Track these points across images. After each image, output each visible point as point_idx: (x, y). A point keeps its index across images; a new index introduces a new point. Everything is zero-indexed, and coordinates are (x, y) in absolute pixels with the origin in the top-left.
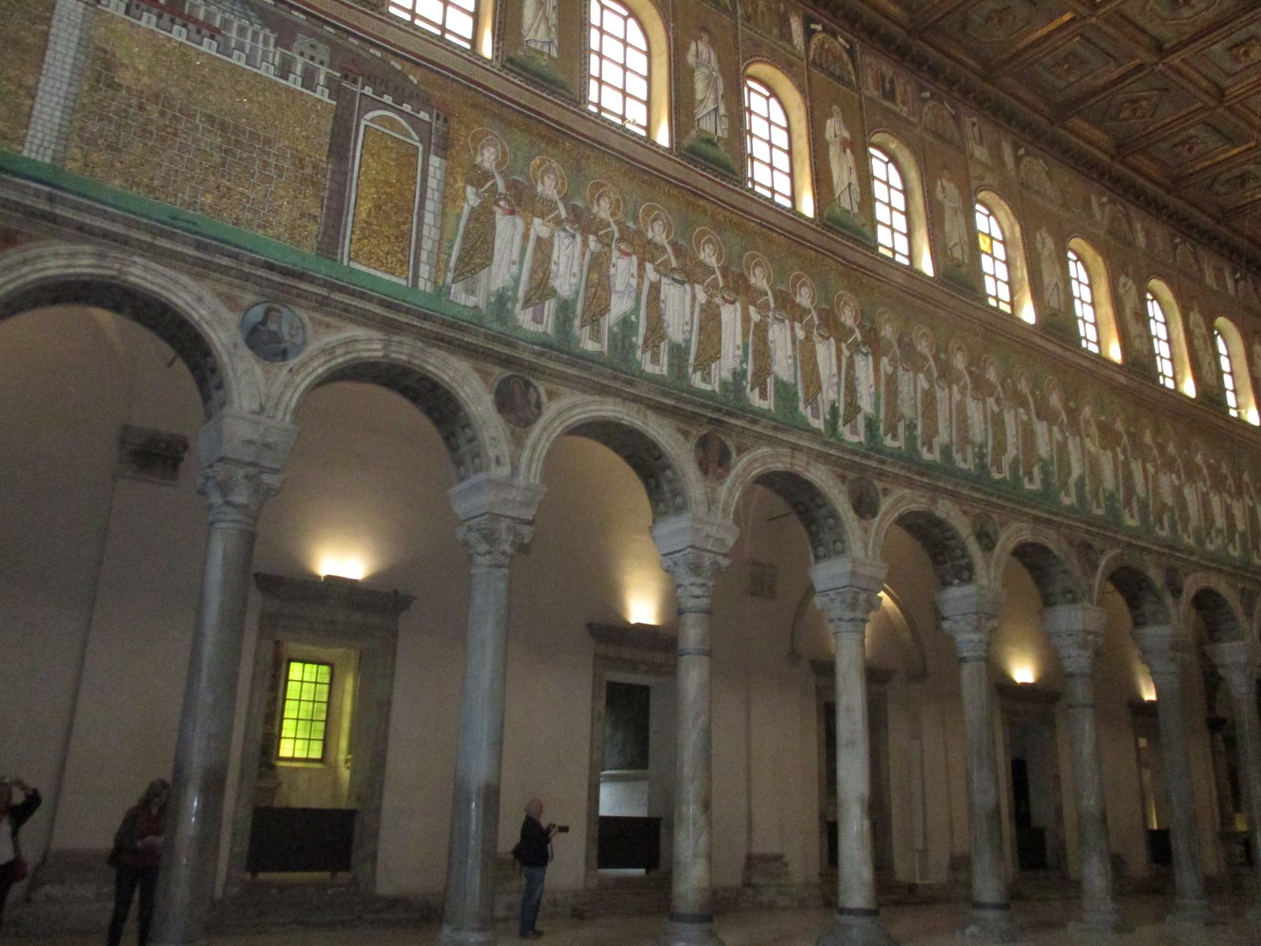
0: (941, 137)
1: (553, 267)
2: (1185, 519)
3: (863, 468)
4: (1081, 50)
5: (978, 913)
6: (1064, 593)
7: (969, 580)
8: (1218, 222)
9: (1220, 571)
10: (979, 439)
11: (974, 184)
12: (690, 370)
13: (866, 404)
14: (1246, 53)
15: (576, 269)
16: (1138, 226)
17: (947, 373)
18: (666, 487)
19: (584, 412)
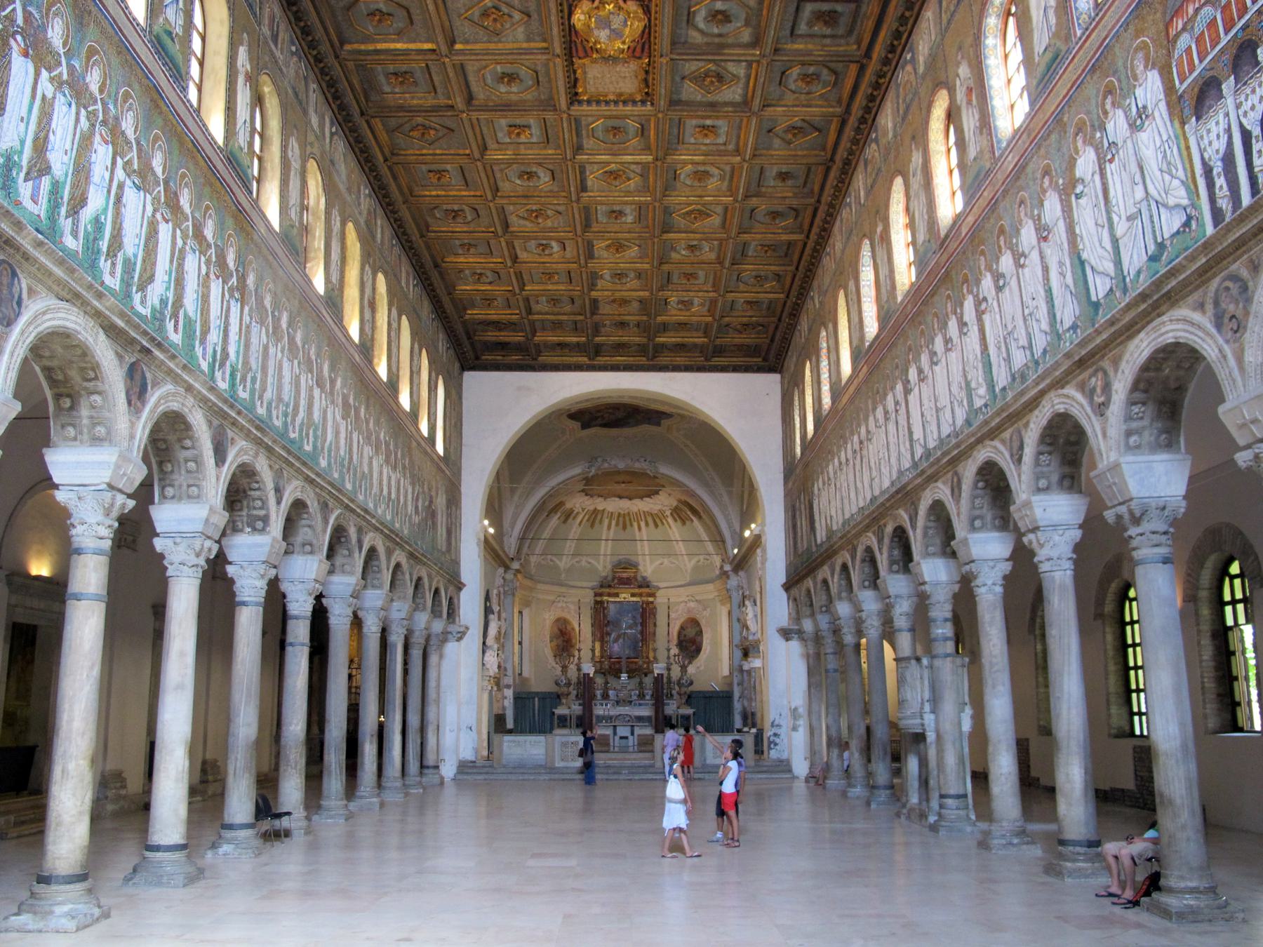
0: (296, 94)
1: (51, 137)
2: (371, 485)
3: (225, 416)
4: (418, 74)
5: (228, 834)
6: (304, 545)
7: (263, 531)
8: (422, 236)
9: (382, 532)
10: (286, 398)
11: (309, 149)
12: (134, 289)
13: (232, 350)
14: (518, 134)
15: (68, 146)
16: (379, 222)
17: (277, 327)
18: (85, 412)
19: (53, 319)
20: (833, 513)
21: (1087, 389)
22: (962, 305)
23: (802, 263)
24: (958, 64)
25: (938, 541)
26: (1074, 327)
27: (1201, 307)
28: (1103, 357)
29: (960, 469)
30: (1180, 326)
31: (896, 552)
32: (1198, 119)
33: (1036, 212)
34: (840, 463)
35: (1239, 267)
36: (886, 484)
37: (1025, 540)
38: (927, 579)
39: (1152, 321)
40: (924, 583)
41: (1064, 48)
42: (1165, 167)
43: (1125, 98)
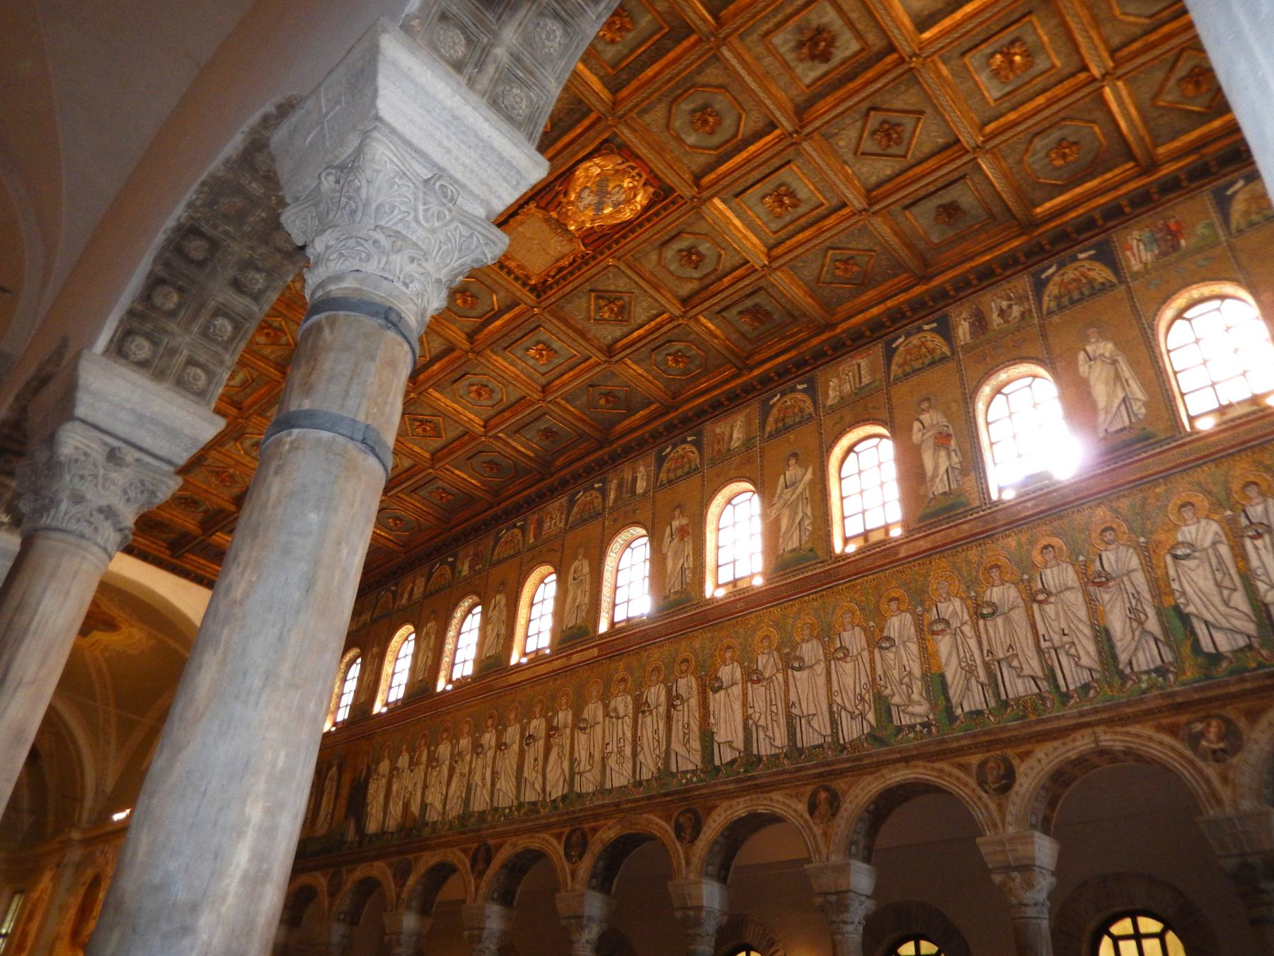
22: (884, 619)
26: (1161, 671)
28: (1225, 705)
29: (839, 784)
31: (601, 864)
33: (1081, 558)
37: (997, 878)
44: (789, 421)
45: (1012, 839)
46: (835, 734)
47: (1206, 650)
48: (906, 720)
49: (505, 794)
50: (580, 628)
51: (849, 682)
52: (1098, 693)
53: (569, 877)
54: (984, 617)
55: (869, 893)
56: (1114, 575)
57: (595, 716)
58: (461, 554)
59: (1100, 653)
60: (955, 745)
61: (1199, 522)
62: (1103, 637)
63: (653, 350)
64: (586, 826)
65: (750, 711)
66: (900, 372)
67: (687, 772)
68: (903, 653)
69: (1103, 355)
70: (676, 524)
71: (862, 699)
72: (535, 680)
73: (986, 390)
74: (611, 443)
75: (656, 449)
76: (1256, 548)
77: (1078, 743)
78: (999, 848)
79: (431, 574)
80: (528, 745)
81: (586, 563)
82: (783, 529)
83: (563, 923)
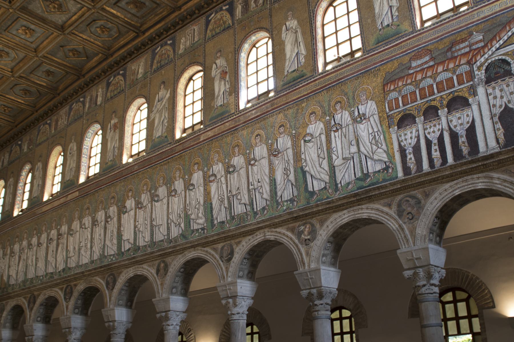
20: (13, 273)
21: (296, 231)
22: (191, 175)
23: (22, 124)
24: (218, 58)
25: (125, 298)
26: (292, 200)
27: (389, 206)
28: (313, 218)
29: (168, 260)
30: (373, 212)
31: (79, 302)
32: (398, 128)
33: (270, 142)
34: (30, 245)
35: (418, 193)
36: (85, 260)
37: (224, 302)
38: (116, 319)
39: (354, 206)
40: (115, 321)
41: (309, 75)
42: (373, 142)
43: (350, 107)
44: (163, 63)
45: (229, 284)
46: (168, 234)
47: (309, 190)
48: (196, 227)
49: (41, 269)
50: (71, 181)
51: (176, 207)
52: (268, 211)
53: (65, 309)
54: (230, 173)
55: (184, 310)
56: (281, 151)
57: (76, 228)
58: (24, 140)
59: (271, 191)
60: (211, 239)
61: (316, 122)
62: (273, 182)
63: (87, 25)
64: (72, 284)
65: (137, 223)
66: (210, 35)
67: (111, 255)
68: (197, 192)
69: (292, 28)
70: (113, 122)
71: (180, 217)
72: (54, 209)
73: (246, 46)
74: (84, 76)
75: (106, 79)
76: (335, 137)
77: (258, 237)
78: (224, 288)
79: (11, 151)
80: (50, 243)
81: (75, 144)
82: (156, 125)
83: (64, 331)
